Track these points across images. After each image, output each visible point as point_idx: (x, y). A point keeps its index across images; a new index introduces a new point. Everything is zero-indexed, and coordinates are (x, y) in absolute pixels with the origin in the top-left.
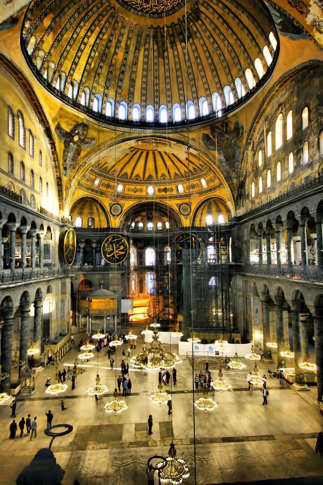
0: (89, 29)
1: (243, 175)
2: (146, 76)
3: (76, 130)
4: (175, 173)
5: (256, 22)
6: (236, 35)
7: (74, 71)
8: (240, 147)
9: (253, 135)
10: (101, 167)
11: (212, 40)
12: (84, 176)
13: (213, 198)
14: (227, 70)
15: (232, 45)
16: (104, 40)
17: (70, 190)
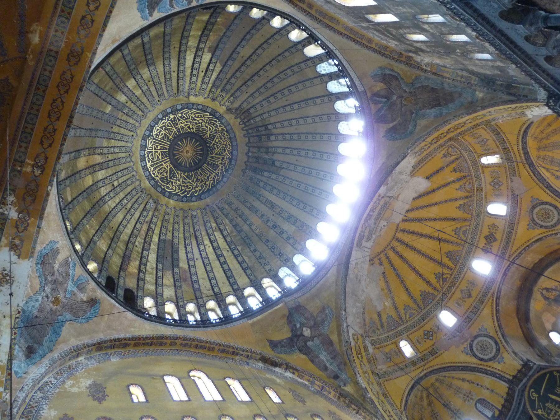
0: (212, 243)
1: (467, 77)
2: (292, 198)
3: (295, 326)
4: (459, 208)
5: (246, 36)
6: (265, 66)
7: (236, 282)
8: (416, 78)
9: (392, 51)
10: (382, 326)
11: (272, 99)
12: (372, 360)
13: (525, 148)
14: (307, 84)
15: (278, 72)
16: (232, 232)
17: (370, 395)
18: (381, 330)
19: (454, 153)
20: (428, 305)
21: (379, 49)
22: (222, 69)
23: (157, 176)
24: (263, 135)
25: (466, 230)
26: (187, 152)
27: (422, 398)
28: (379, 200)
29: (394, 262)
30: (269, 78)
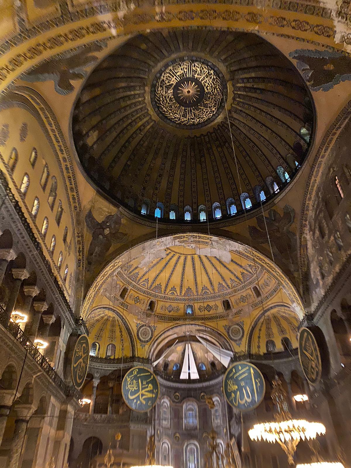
3: (107, 223)
9: (307, 214)
10: (131, 272)
13: (271, 308)
15: (267, 138)
18: (128, 273)
19: (253, 270)
20: (154, 291)
21: (306, 206)
22: (259, 99)
23: (164, 77)
24: (219, 141)
25: (208, 293)
26: (189, 92)
27: (99, 315)
28: (208, 238)
29: (172, 261)
30: (261, 134)
